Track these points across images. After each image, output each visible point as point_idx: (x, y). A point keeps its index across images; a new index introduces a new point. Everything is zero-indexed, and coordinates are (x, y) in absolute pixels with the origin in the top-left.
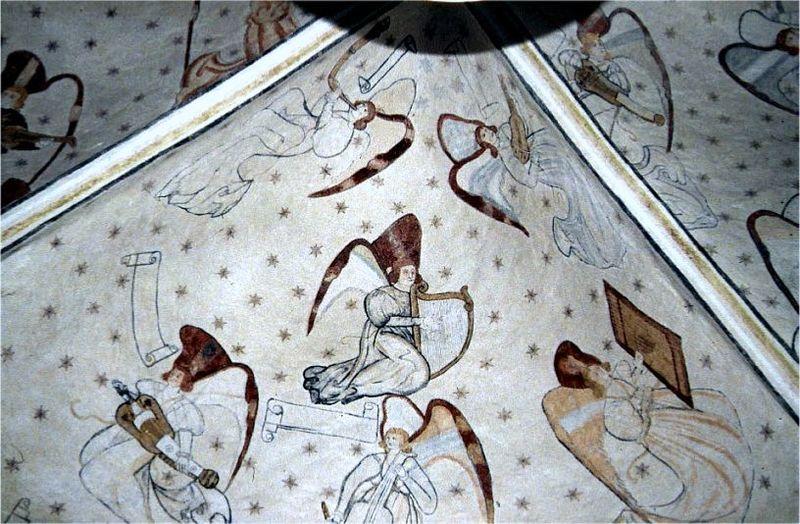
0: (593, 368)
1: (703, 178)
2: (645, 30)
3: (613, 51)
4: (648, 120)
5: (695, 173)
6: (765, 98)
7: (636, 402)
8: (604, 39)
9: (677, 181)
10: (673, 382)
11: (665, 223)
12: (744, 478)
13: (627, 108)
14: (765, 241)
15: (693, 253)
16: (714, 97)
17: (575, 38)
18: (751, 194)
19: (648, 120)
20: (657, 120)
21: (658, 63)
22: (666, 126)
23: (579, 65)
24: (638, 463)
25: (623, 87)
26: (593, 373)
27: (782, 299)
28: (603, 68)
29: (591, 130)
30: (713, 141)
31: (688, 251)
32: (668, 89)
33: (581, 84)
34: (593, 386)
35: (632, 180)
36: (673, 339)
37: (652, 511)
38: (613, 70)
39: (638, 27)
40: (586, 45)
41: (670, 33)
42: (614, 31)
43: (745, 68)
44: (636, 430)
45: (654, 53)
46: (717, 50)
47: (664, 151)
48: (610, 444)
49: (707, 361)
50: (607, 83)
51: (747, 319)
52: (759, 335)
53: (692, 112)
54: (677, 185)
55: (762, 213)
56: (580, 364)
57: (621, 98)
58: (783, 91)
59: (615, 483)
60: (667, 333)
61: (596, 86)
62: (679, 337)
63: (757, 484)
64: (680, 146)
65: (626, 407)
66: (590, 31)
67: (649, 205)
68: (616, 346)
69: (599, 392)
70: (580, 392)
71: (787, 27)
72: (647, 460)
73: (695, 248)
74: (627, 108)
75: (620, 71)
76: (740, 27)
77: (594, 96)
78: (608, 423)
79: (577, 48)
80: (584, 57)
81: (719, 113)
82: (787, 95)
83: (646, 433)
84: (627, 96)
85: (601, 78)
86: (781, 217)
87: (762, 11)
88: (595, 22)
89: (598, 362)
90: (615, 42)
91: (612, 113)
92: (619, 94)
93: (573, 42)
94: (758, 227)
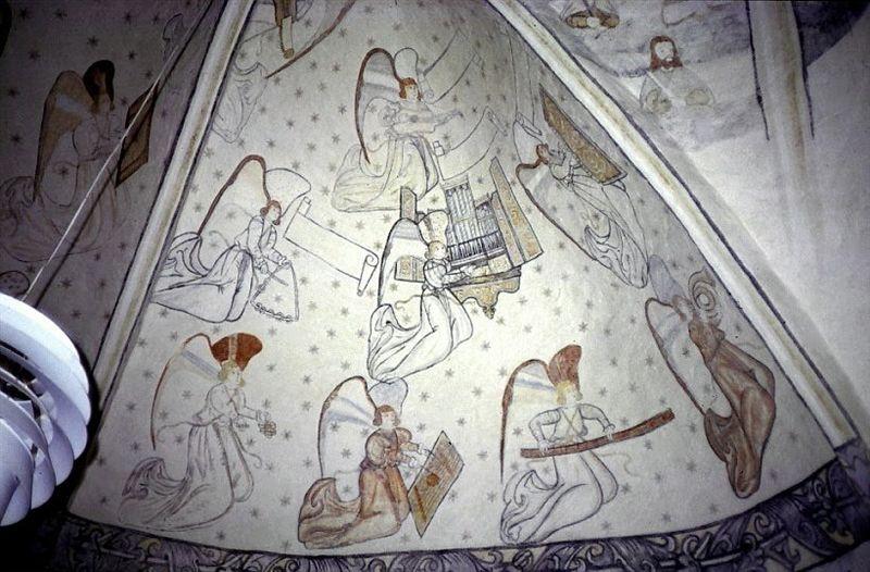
0: (106, 96)
4: (282, 48)
7: (102, 143)
10: (123, 166)
11: (198, 128)
12: (93, 243)
13: (281, 33)
19: (282, 48)
20: (287, 54)
22: (287, 61)
24: (67, 166)
25: (298, 15)
26: (104, 97)
34: (96, 103)
36: (144, 157)
37: (43, 194)
44: (86, 152)
46: (377, 45)
47: (264, 75)
48: (65, 141)
51: (169, 212)
52: (163, 224)
54: (244, 101)
55: (261, 160)
56: (104, 87)
57: (287, 22)
59: (44, 159)
60: (146, 150)
63: (95, 252)
65: (94, 137)
69: (95, 109)
70: (87, 96)
72: (72, 170)
74: (281, 33)
77: (273, 7)
78: (80, 129)
83: (87, 160)
86: (265, 172)
89: (112, 99)
92: (289, 19)
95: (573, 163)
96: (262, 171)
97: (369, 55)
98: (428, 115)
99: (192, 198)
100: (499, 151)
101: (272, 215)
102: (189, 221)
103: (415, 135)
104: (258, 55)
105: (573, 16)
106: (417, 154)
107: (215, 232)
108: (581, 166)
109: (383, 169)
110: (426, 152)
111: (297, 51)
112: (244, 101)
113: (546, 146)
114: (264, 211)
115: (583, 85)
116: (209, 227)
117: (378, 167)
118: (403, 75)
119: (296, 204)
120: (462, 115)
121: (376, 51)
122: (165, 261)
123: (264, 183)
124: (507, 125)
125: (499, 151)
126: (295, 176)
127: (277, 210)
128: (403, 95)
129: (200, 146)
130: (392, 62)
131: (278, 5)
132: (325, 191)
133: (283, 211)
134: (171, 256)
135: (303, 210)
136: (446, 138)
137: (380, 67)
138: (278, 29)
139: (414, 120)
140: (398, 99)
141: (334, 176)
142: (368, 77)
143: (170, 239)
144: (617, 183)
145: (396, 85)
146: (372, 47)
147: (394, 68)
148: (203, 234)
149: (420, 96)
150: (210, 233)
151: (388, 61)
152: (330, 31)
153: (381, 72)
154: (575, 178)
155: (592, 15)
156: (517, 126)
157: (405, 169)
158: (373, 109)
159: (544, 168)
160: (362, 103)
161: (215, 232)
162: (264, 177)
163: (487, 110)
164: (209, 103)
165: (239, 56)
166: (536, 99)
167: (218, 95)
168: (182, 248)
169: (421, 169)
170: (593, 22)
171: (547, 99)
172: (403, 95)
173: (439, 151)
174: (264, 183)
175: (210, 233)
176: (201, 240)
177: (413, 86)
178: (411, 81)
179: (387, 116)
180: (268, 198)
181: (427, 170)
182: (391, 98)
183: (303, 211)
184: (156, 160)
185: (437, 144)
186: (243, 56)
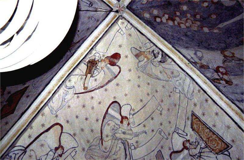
1: (69, 107)
2: (116, 77)
3: (105, 69)
4: (84, 85)
5: (70, 104)
6: (104, 118)
8: (109, 65)
9: (65, 99)
11: (45, 99)
14: (51, 130)
15: (37, 110)
16: (100, 103)
17: (105, 56)
18: (68, 122)
19: (84, 85)
20: (85, 88)
21: (106, 83)
22: (83, 91)
23: (96, 60)
27: (32, 139)
28: (98, 67)
29: (70, 69)
30: (84, 106)
31: (37, 108)
32: (98, 88)
33: (89, 62)
35: (56, 85)
38: (98, 70)
39: (116, 75)
40: (104, 60)
41: (118, 85)
42: (112, 68)
43: (113, 110)
45: (109, 81)
49: (7, 123)
50: (93, 70)
51: (18, 131)
52: (14, 135)
53: (92, 98)
54: (64, 99)
55: (62, 127)
57: (89, 75)
58: (108, 123)
61: (90, 67)
62: (13, 113)
64: (78, 97)
66: (109, 60)
67: (49, 93)
68: (10, 95)
71: (129, 118)
73: (39, 109)
75: (99, 73)
76: (125, 105)
77: (87, 67)
79: (102, 58)
80: (100, 60)
81: (95, 106)
82: (107, 124)
84: (91, 77)
85: (94, 68)
86: (62, 132)
87: (132, 110)
88: (113, 61)
90: (108, 69)
91: (83, 74)
92: (90, 75)
93: (103, 56)
94: (56, 126)
95: (203, 145)
96: (60, 131)
97: (113, 102)
98: (130, 132)
99: (29, 131)
100: (162, 147)
101: (59, 151)
102: (24, 141)
103: (124, 139)
104: (75, 83)
105: (214, 79)
106: (123, 147)
107: (33, 150)
108: (207, 147)
109: (108, 149)
110: (127, 147)
111: (89, 89)
112: (64, 99)
113: (189, 141)
114: (56, 149)
115: (222, 99)
116: (31, 147)
117: (106, 149)
118: (123, 114)
119: (69, 151)
120: (146, 133)
121: (116, 102)
122: (6, 156)
123: (60, 137)
124: (169, 134)
125: (162, 147)
126: (73, 139)
127: (62, 150)
128: (122, 122)
129: (43, 107)
130: (121, 108)
131: (89, 67)
132: (84, 150)
133: (64, 152)
134: (10, 155)
135: (73, 154)
136: (137, 142)
137: (115, 109)
138: (85, 77)
139: (124, 133)
140: (119, 123)
141: (88, 145)
142: (110, 111)
143: (13, 145)
144: (226, 153)
145: (120, 118)
146: (115, 100)
147: (120, 111)
148: (28, 150)
149: (129, 124)
150: (31, 150)
151: (119, 108)
152: (102, 87)
153: (115, 111)
154: (202, 154)
155: (222, 80)
156: (175, 134)
157: (117, 152)
158: (109, 125)
159: (186, 152)
160: (105, 121)
161: (33, 150)
162: (61, 134)
163: (160, 130)
164: (53, 90)
165: (68, 80)
166: (188, 119)
167: (58, 88)
168: (16, 152)
169: (123, 154)
170: (223, 82)
171: (194, 117)
172: (122, 122)
173: (133, 148)
174: (60, 137)
175: (31, 150)
176: (26, 152)
177: (127, 120)
178: (126, 118)
179: (113, 129)
180: (60, 144)
181: (126, 155)
182: (117, 122)
183: (73, 154)
184: (17, 113)
185: (132, 145)
186: (70, 81)
